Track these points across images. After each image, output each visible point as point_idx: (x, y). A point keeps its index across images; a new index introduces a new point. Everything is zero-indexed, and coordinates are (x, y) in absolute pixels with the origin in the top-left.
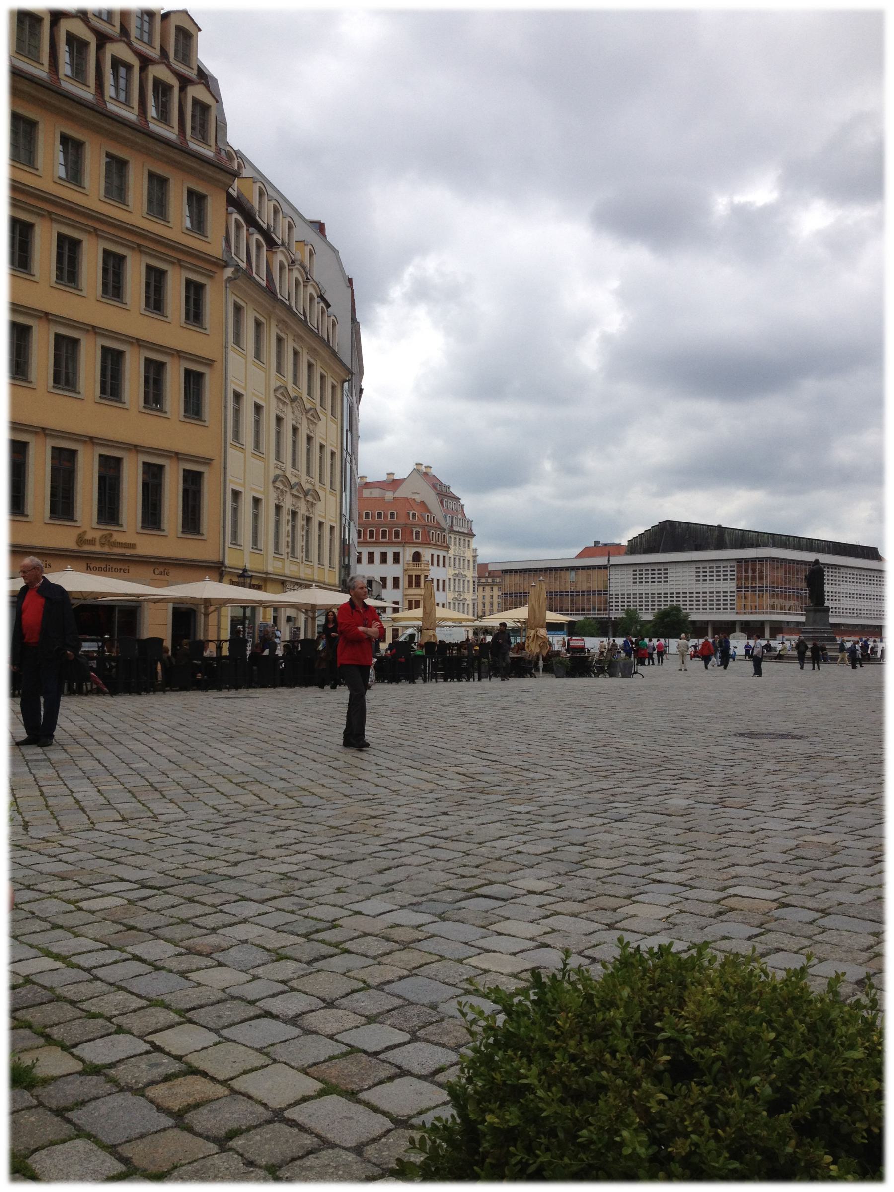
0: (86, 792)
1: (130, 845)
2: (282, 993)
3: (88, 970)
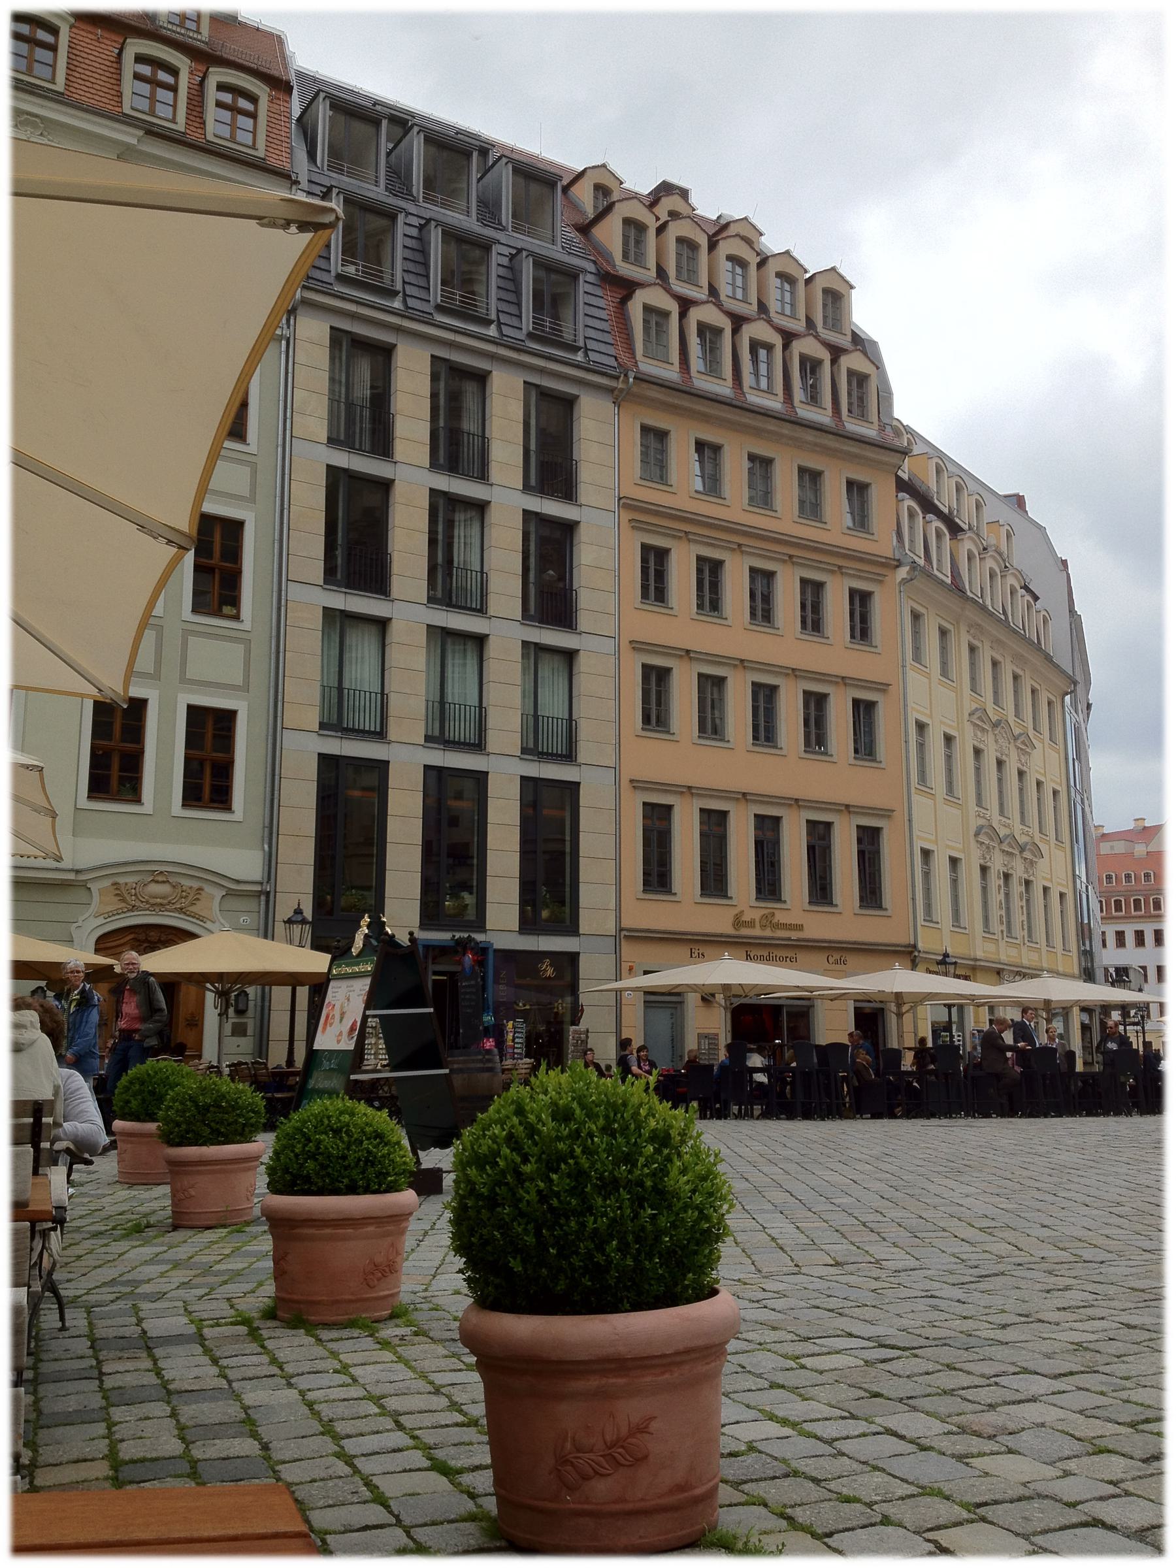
1: (853, 1294)
2: (1114, 1496)
3: (830, 1442)
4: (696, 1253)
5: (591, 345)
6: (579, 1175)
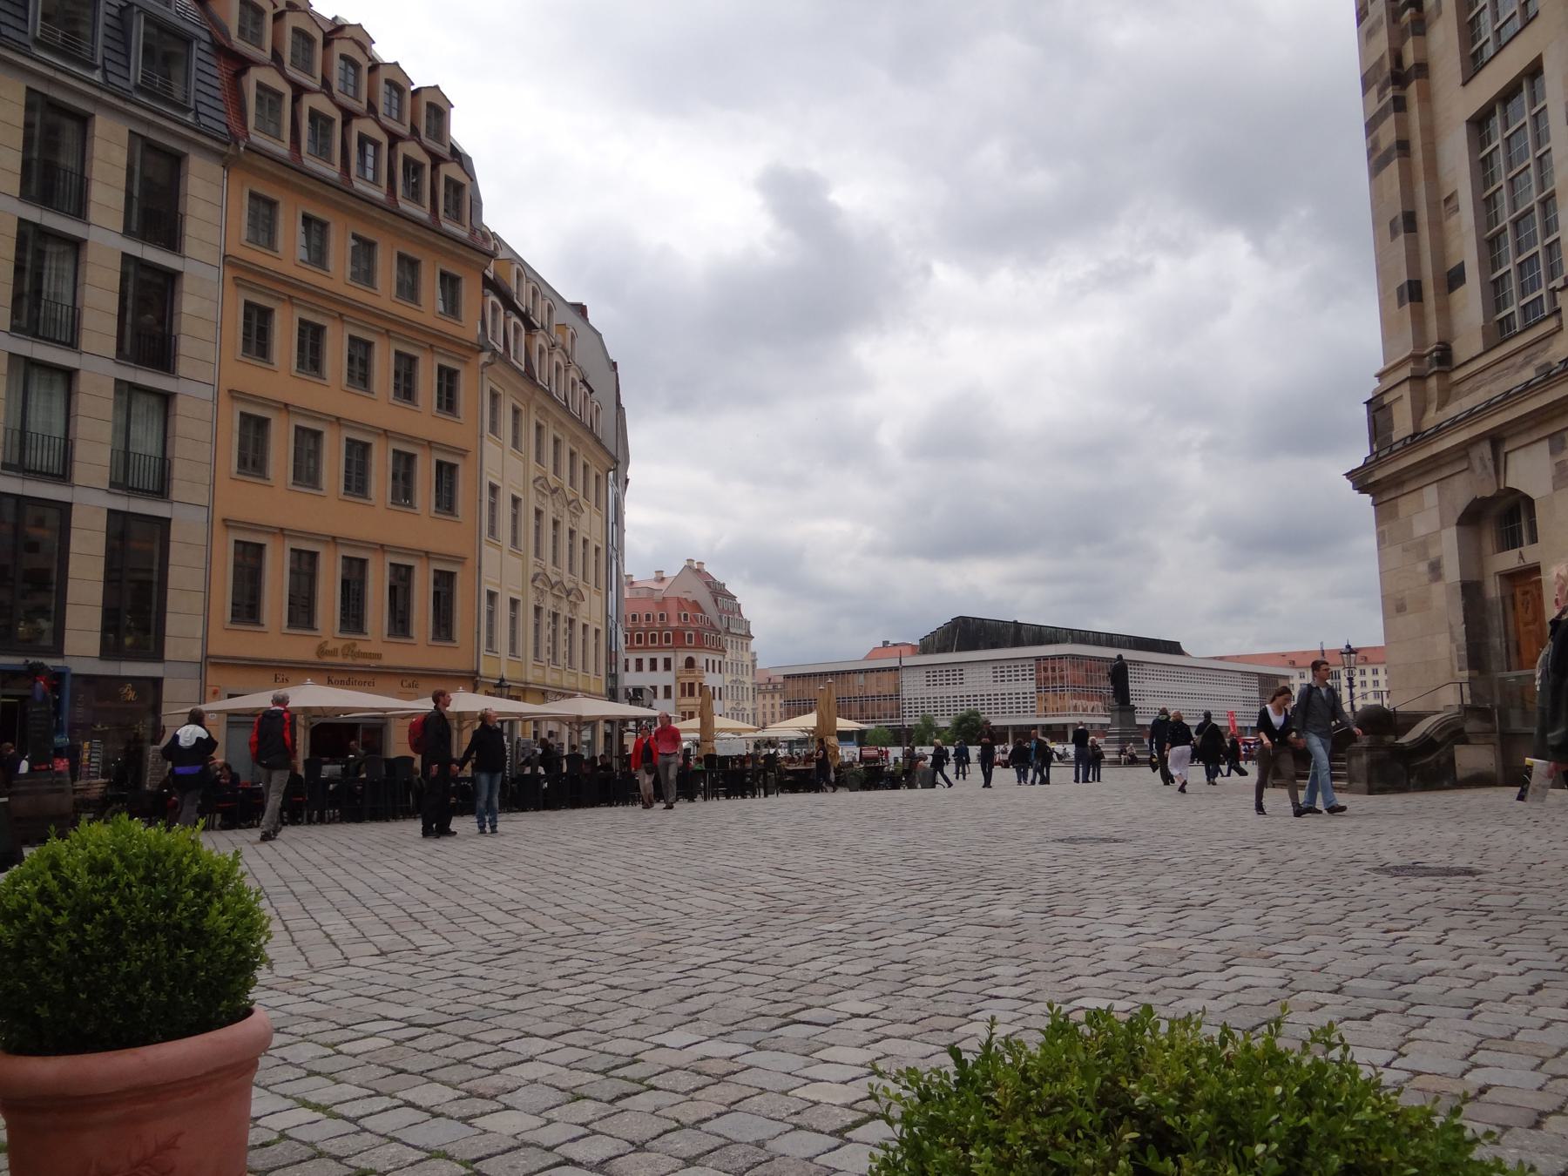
0: (336, 925)
1: (392, 980)
2: (583, 1136)
3: (354, 1121)
4: (232, 982)
5: (202, 108)
6: (114, 924)
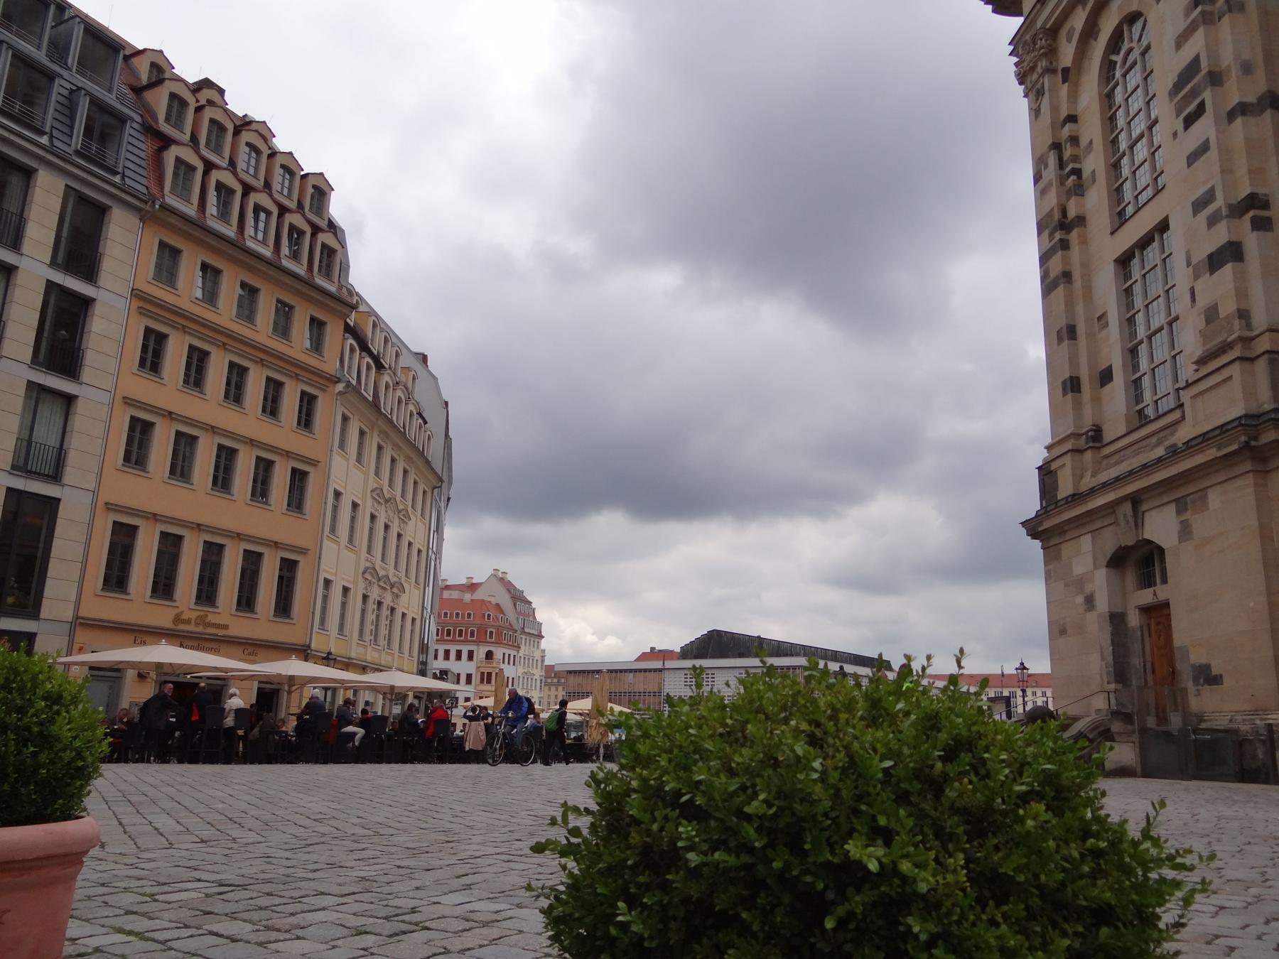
0: (163, 822)
4: (69, 785)
5: (128, 173)
